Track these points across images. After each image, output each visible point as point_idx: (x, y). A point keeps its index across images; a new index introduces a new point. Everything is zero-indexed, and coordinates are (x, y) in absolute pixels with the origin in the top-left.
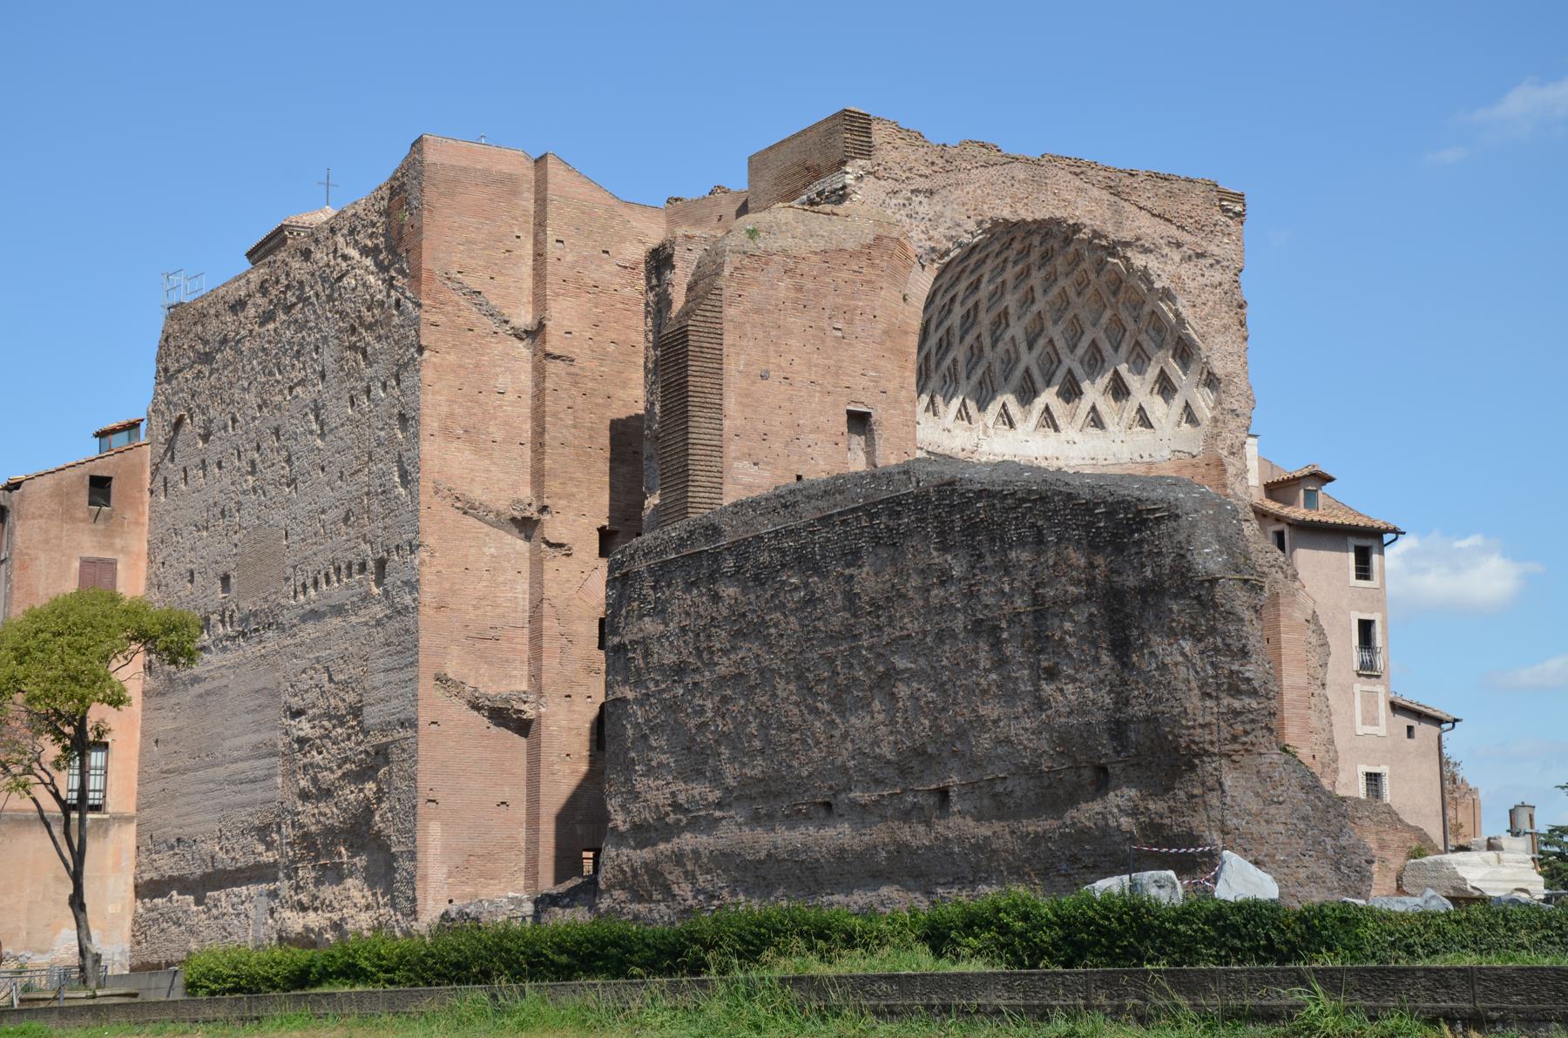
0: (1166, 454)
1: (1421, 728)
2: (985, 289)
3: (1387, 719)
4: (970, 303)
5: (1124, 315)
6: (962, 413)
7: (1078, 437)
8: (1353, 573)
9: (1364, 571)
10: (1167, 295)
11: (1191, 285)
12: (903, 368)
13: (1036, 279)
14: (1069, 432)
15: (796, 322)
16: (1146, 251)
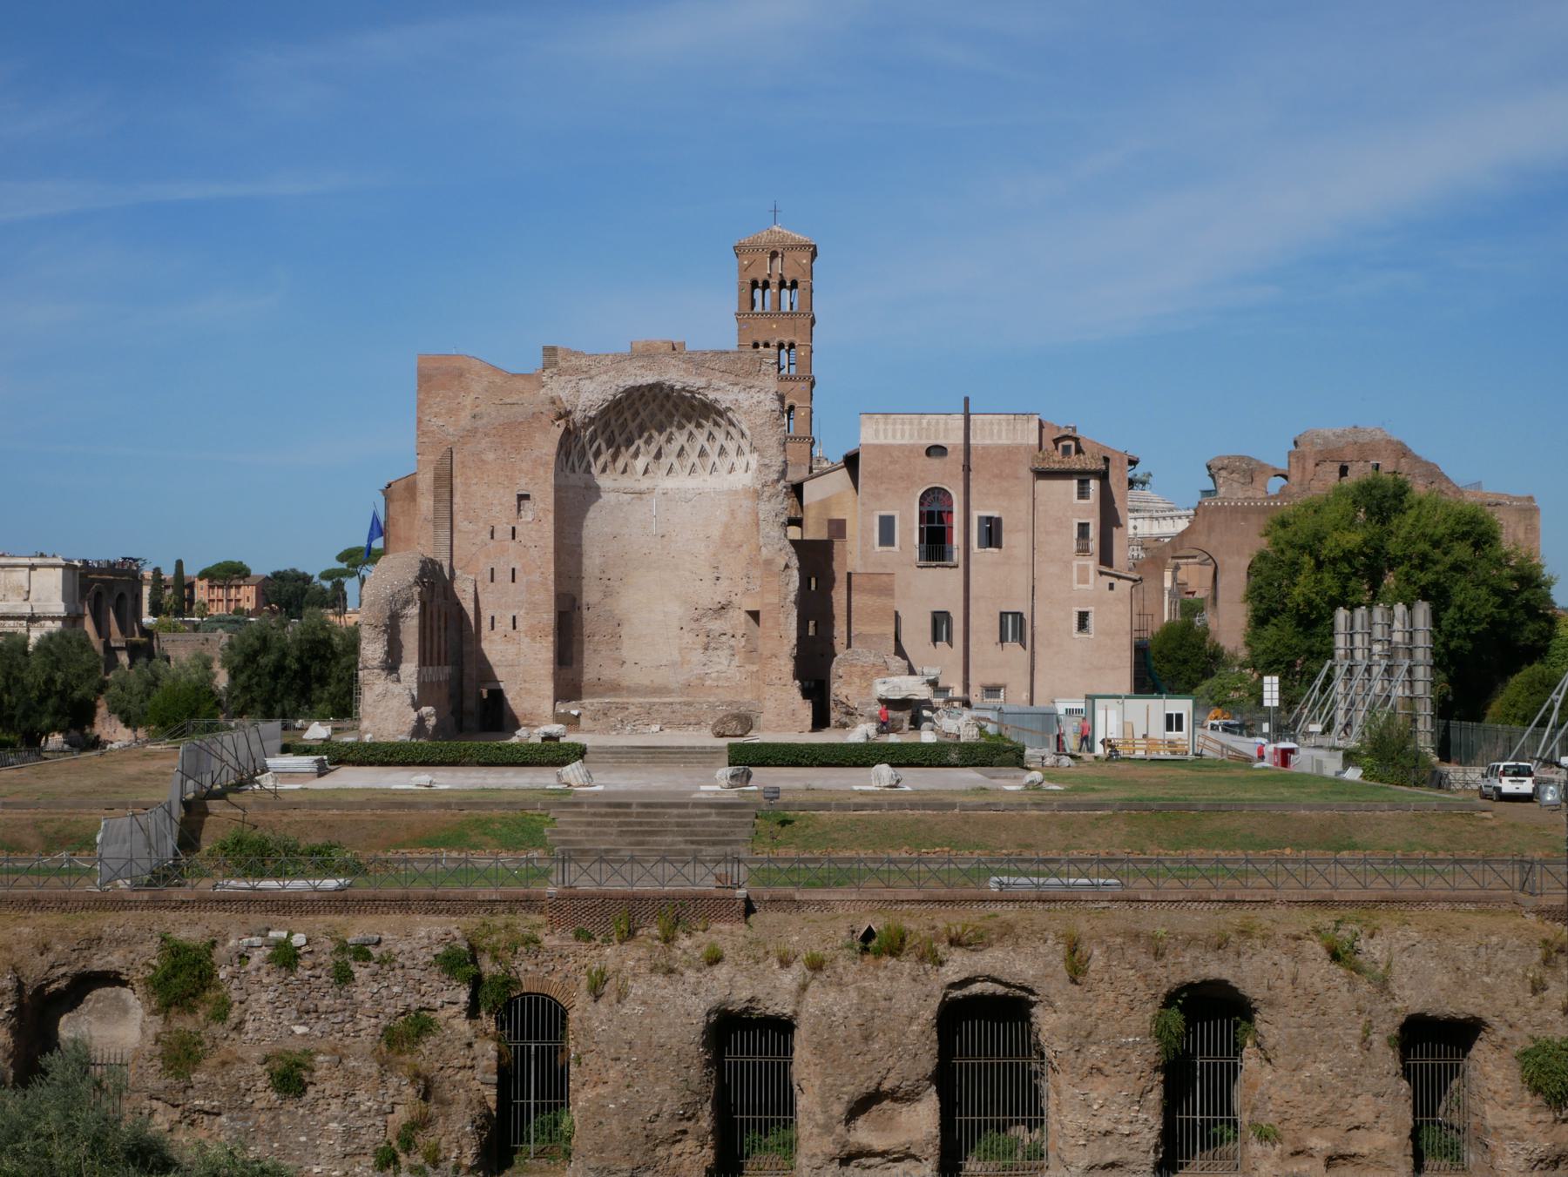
0: (741, 486)
1: (1118, 583)
2: (643, 414)
3: (1095, 581)
4: (638, 421)
5: (719, 419)
6: (646, 471)
7: (708, 478)
8: (1076, 496)
9: (1083, 494)
10: (729, 409)
11: (746, 405)
12: (546, 472)
13: (669, 406)
14: (706, 476)
15: (490, 456)
16: (715, 390)
